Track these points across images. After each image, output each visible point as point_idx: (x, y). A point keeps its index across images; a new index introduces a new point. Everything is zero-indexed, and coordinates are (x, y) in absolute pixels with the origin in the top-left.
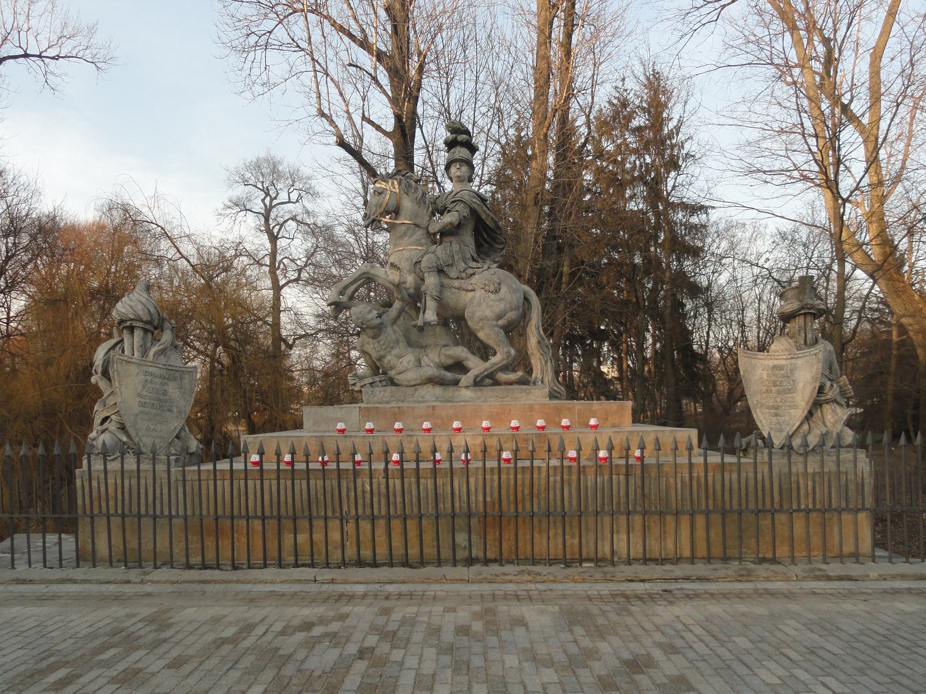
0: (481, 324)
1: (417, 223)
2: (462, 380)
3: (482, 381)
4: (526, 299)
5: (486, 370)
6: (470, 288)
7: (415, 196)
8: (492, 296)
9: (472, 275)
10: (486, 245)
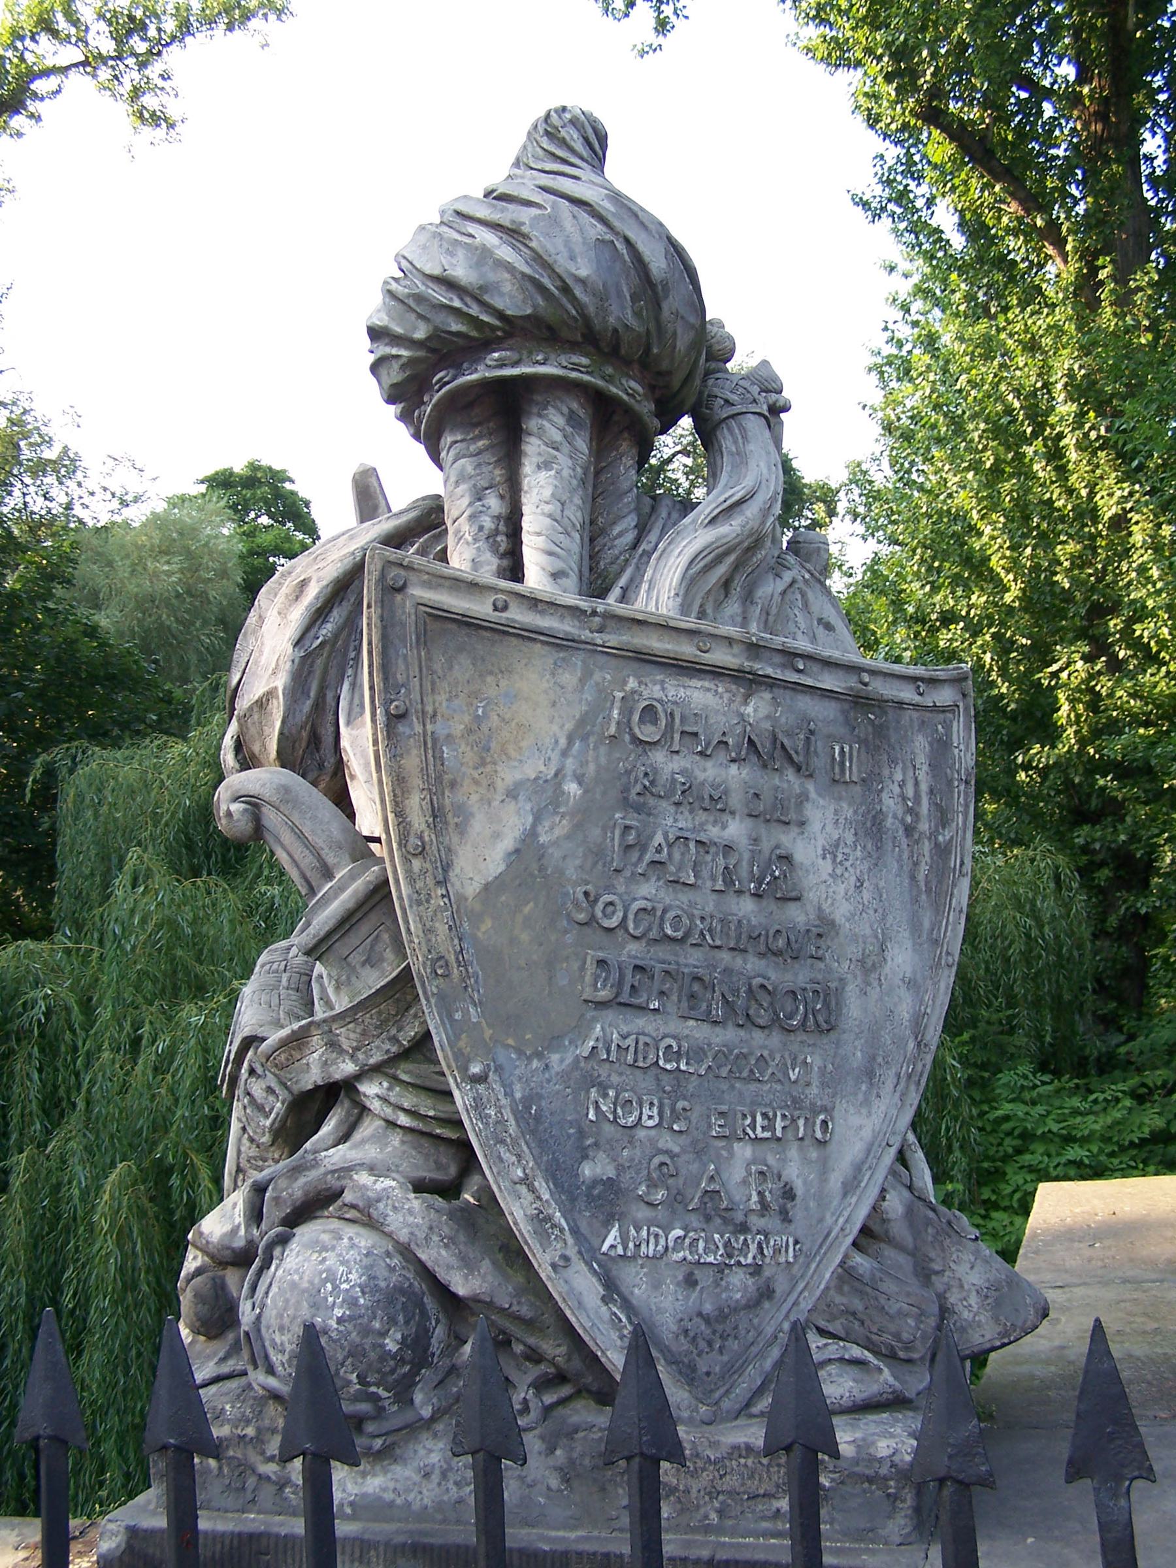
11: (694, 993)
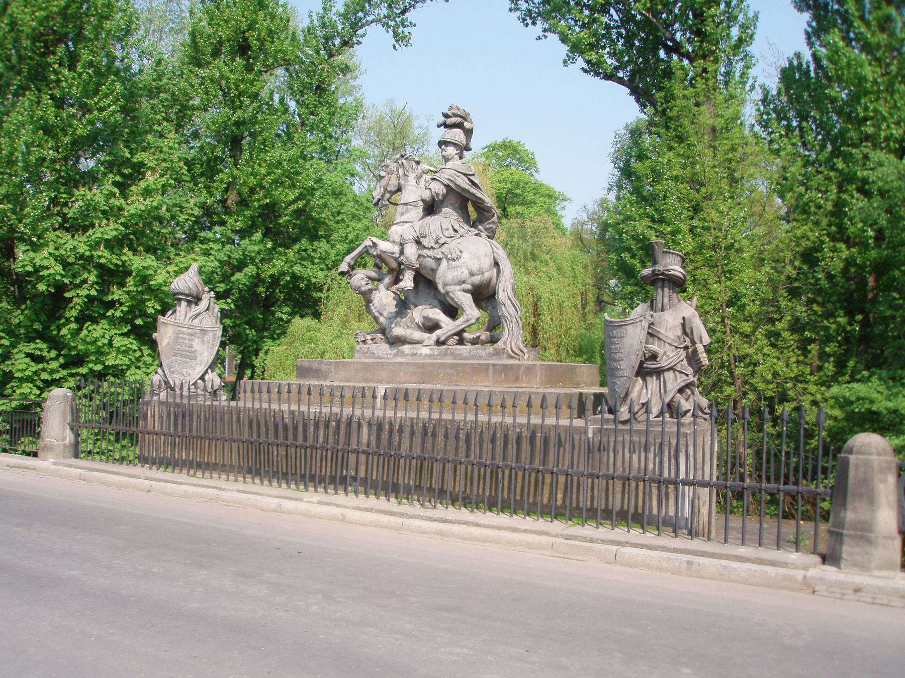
6: (440, 256)
11: (182, 355)
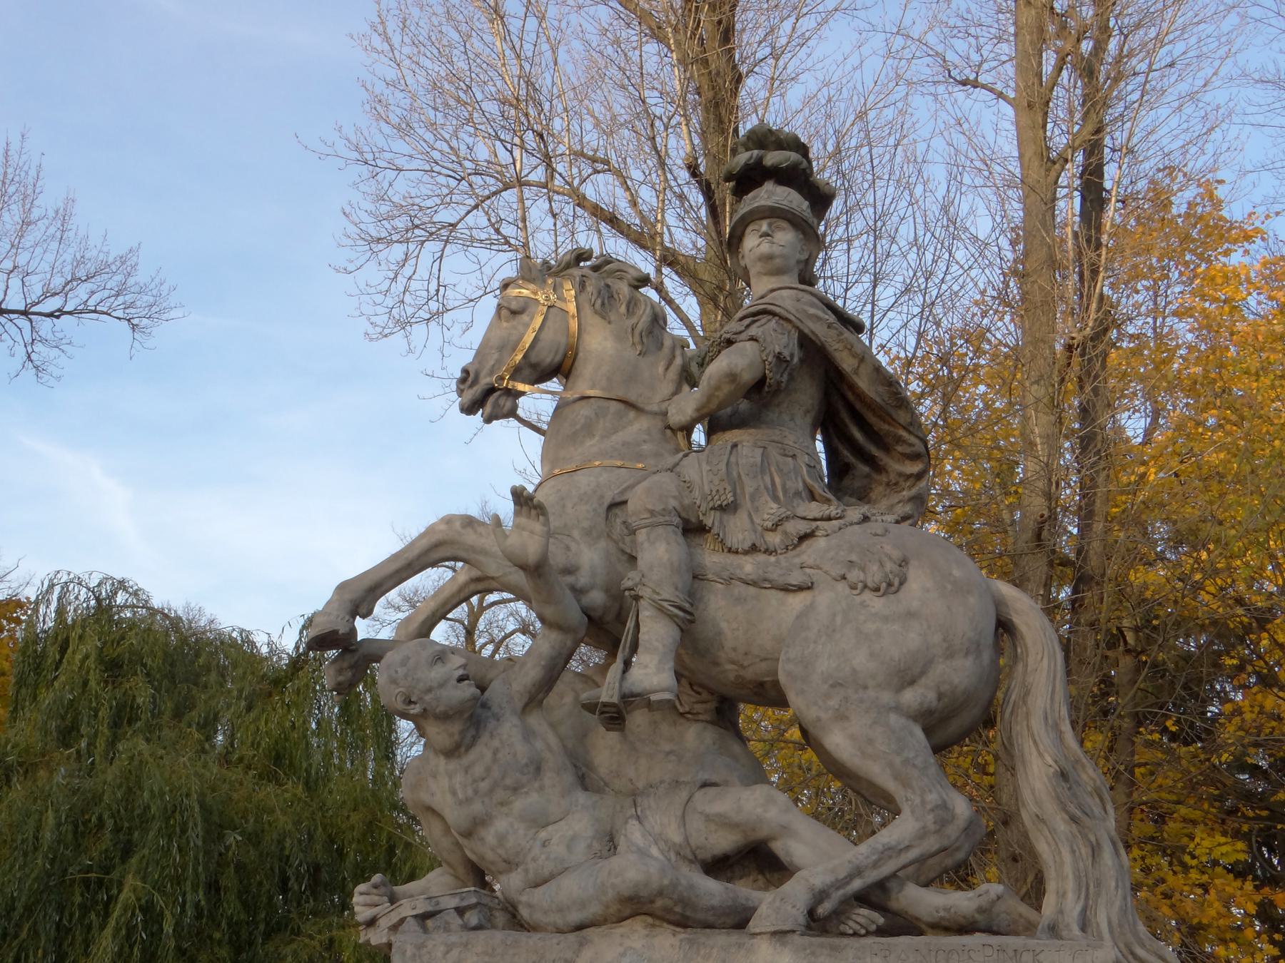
0: (834, 703)
1: (632, 397)
2: (763, 910)
3: (839, 913)
4: (1004, 627)
5: (858, 872)
6: (796, 578)
7: (630, 322)
8: (877, 604)
9: (803, 538)
10: (864, 469)
